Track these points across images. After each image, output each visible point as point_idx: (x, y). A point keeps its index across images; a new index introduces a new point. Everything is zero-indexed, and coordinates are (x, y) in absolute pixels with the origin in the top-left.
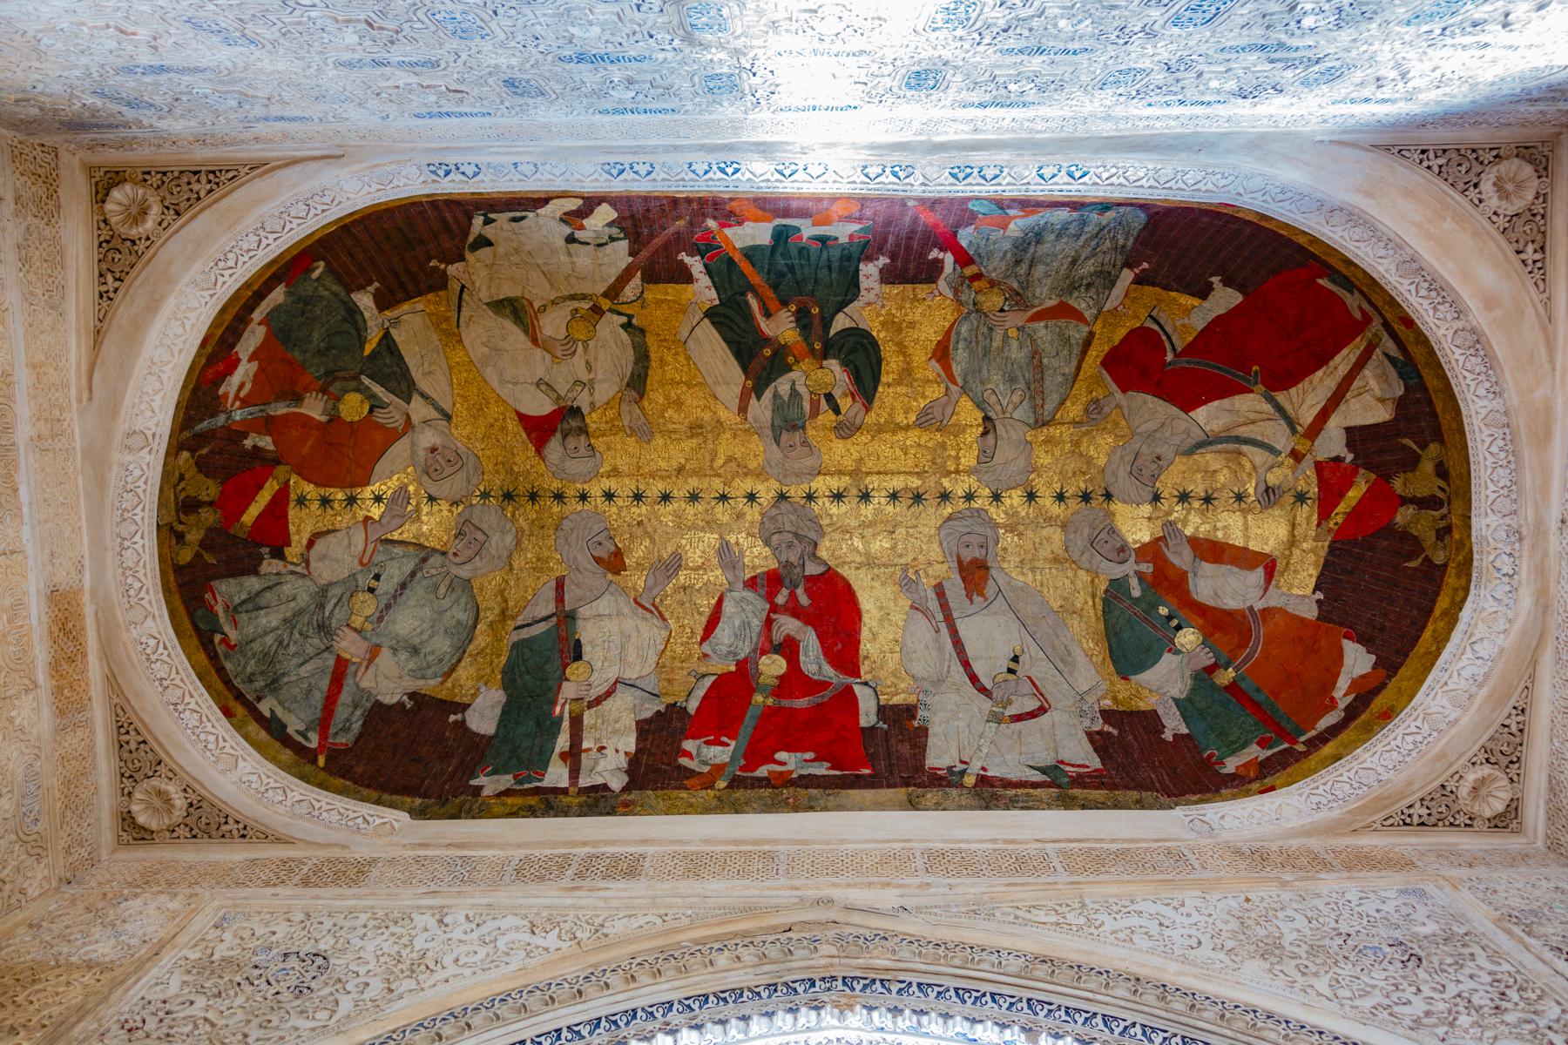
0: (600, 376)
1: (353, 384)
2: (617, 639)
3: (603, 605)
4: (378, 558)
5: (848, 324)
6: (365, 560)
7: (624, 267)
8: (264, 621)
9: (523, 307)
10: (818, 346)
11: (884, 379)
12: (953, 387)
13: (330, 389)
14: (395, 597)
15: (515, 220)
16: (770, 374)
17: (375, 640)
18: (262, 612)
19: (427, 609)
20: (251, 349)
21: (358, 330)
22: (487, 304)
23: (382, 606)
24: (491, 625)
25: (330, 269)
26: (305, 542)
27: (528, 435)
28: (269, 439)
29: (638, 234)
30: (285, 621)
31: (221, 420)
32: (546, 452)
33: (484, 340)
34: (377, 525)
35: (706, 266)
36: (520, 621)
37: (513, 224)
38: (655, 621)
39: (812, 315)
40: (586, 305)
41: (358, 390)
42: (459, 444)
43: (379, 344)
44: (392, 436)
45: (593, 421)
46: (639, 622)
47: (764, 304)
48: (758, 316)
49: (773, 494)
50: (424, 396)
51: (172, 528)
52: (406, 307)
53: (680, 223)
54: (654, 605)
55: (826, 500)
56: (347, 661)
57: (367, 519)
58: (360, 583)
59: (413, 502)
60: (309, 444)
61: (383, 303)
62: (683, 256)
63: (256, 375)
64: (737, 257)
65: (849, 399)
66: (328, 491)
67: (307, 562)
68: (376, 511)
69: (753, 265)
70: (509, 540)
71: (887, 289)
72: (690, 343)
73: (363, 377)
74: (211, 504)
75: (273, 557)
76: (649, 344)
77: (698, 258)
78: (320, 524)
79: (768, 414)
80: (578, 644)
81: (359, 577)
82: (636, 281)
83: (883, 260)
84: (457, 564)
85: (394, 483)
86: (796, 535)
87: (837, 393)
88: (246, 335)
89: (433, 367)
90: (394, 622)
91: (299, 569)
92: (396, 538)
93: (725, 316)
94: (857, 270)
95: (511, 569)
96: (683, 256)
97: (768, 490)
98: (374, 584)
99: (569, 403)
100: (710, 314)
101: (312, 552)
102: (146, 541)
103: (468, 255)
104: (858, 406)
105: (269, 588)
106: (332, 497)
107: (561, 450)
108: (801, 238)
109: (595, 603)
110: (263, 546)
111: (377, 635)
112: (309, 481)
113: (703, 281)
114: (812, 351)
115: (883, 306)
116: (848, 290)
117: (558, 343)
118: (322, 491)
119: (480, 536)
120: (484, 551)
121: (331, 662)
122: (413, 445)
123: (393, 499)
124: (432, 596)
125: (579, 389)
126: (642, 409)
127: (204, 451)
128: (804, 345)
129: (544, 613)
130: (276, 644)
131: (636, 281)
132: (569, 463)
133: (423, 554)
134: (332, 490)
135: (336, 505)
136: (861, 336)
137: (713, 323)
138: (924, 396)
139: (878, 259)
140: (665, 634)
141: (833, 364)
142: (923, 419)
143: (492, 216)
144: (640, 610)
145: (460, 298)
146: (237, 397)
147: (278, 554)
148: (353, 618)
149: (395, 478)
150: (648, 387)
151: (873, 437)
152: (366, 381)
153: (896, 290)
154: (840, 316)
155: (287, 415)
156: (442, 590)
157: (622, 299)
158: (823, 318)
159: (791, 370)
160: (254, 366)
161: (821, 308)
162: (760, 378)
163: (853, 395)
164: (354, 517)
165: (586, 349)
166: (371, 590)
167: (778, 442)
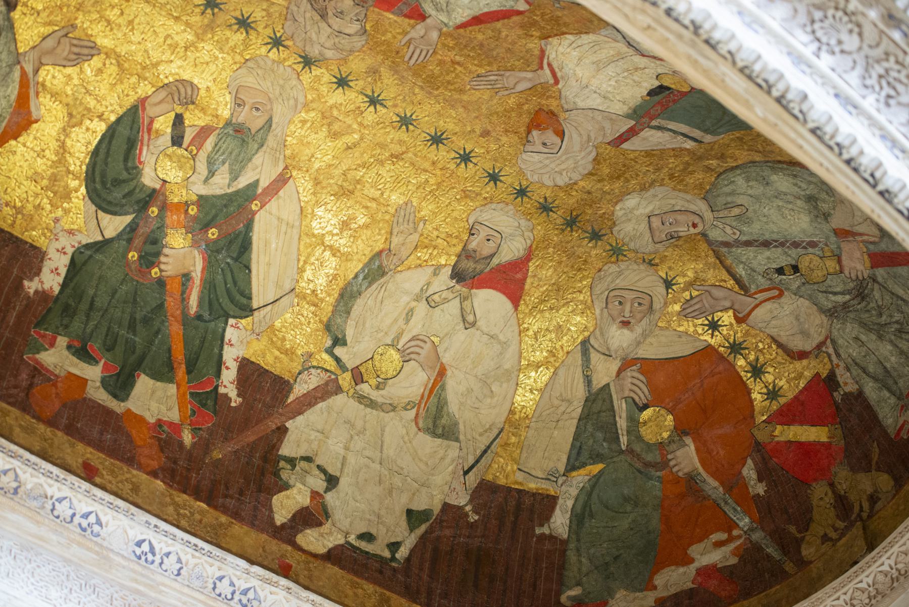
0: (405, 299)
1: (637, 448)
2: (611, 70)
3: (595, 102)
4: (763, 282)
5: (105, 218)
6: (776, 293)
7: (300, 419)
8: (893, 359)
9: (426, 417)
10: (154, 211)
11: (101, 128)
12: (29, 69)
13: (659, 460)
14: (782, 244)
15: (367, 537)
16: (226, 206)
17: (833, 239)
18: (888, 365)
19: (765, 211)
20: (682, 570)
21: (590, 495)
22: (457, 440)
23: (800, 251)
24: (722, 157)
25: (562, 585)
26: (805, 362)
27: (525, 279)
28: (745, 472)
29: (265, 459)
30: (880, 337)
31: (757, 536)
32: (522, 253)
33: (489, 400)
34: (736, 307)
35: (218, 374)
36: (689, 145)
37: (373, 531)
38: (552, 56)
39: (139, 251)
40: (364, 388)
41: (639, 438)
42: (598, 312)
43: (584, 465)
44: (648, 367)
45: (447, 260)
46: (571, 66)
47: (183, 293)
48: (197, 282)
49: (316, 71)
50: (588, 381)
51: (870, 517)
52: (532, 486)
53: (217, 455)
54: (541, 68)
55: (260, 29)
56: (869, 255)
57: (740, 320)
58: (798, 283)
59: (687, 295)
60: (720, 432)
61: (547, 503)
62: (235, 400)
63: (700, 540)
64: (181, 371)
65: (156, 125)
66: (746, 376)
67: (819, 346)
68: (727, 318)
69: (169, 350)
70: (631, 202)
71: (42, 242)
72: (288, 286)
73: (624, 448)
74: (832, 485)
75: (837, 385)
76: (330, 308)
77: (222, 390)
78: (779, 359)
79: (258, 159)
80: (651, 93)
81: (794, 286)
82: (300, 389)
83: (31, 286)
84: (703, 221)
85: (687, 326)
86: (323, 16)
87: (167, 139)
88: (673, 591)
89: (556, 402)
90: (804, 231)
91: (831, 351)
92: (732, 282)
93: (232, 300)
94: (64, 286)
95: (654, 181)
96: (235, 400)
97: (318, 79)
98: (787, 270)
99: (458, 287)
100: (247, 310)
101: (808, 346)
102: (883, 559)
103: (437, 509)
104: (151, 111)
105: (864, 370)
106: (748, 368)
107: (504, 247)
108: (106, 368)
109: (600, 108)
110: (835, 402)
111: (827, 238)
112: (751, 401)
113: (230, 356)
114: (164, 207)
115: (56, 220)
116: (85, 263)
117: (421, 358)
118: (750, 383)
119: (656, 222)
120: (665, 210)
121: (880, 272)
122: (639, 343)
123: (702, 313)
124: (750, 214)
125: (436, 297)
126: (388, 240)
127: (792, 529)
128: (168, 221)
129: (659, 134)
130: (903, 336)
131: (300, 389)
132: (506, 231)
133: (724, 250)
134: (743, 374)
135: (752, 357)
136: (99, 196)
137: (250, 298)
138: (69, 78)
139: (36, 292)
140: (554, 41)
141: (148, 179)
142: (86, 51)
143: (387, 554)
144: (559, 75)
145: (477, 462)
146: (730, 539)
147: (831, 381)
148: (831, 270)
149: (681, 329)
150: (365, 260)
151: (156, 65)
152: (624, 440)
153: (35, 236)
154: (110, 233)
155: (714, 475)
156: (736, 211)
157: (325, 376)
158: (130, 241)
159: (201, 197)
160: (694, 551)
161: (125, 256)
162: (240, 206)
163: (149, 130)
164: (747, 334)
165: (398, 338)
166: (796, 269)
167: (270, 121)
